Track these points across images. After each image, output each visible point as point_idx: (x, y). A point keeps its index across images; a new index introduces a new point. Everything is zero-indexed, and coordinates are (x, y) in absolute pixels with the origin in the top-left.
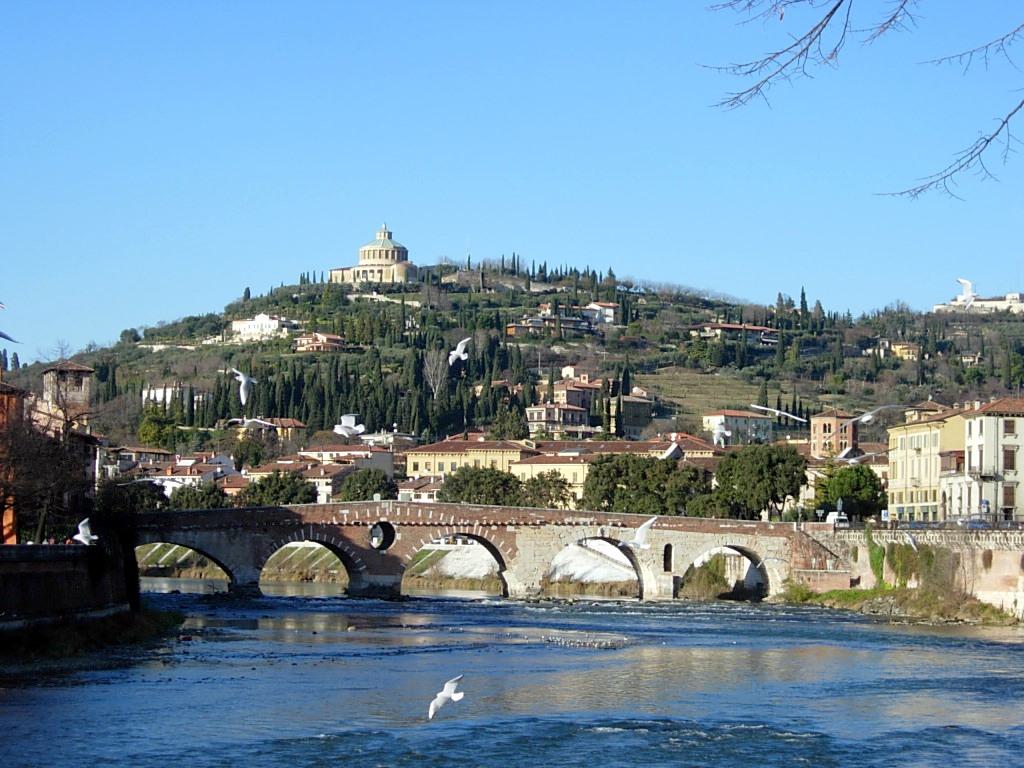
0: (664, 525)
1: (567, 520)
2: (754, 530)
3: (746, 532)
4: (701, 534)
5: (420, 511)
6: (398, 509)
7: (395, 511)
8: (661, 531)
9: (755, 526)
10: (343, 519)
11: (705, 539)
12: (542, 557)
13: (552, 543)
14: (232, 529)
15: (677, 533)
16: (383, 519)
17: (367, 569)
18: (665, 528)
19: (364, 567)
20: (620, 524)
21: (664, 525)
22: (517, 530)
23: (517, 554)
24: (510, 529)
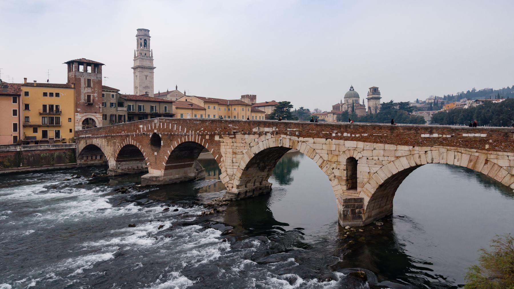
0: (345, 134)
1: (254, 130)
2: (483, 141)
3: (469, 144)
4: (392, 147)
5: (170, 124)
6: (161, 123)
7: (160, 125)
8: (341, 142)
9: (484, 135)
10: (140, 131)
11: (399, 154)
12: (237, 164)
13: (244, 152)
14: (108, 138)
15: (361, 144)
16: (155, 131)
17: (150, 164)
18: (347, 139)
19: (149, 163)
20: (297, 133)
21: (345, 134)
22: (221, 139)
23: (222, 160)
24: (217, 138)
